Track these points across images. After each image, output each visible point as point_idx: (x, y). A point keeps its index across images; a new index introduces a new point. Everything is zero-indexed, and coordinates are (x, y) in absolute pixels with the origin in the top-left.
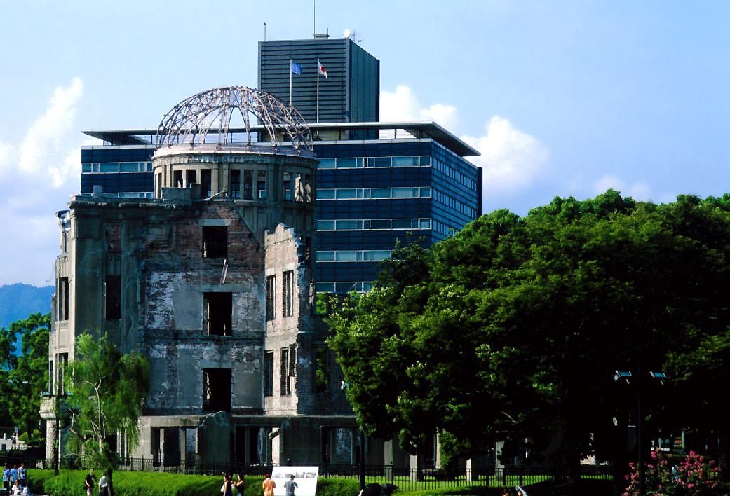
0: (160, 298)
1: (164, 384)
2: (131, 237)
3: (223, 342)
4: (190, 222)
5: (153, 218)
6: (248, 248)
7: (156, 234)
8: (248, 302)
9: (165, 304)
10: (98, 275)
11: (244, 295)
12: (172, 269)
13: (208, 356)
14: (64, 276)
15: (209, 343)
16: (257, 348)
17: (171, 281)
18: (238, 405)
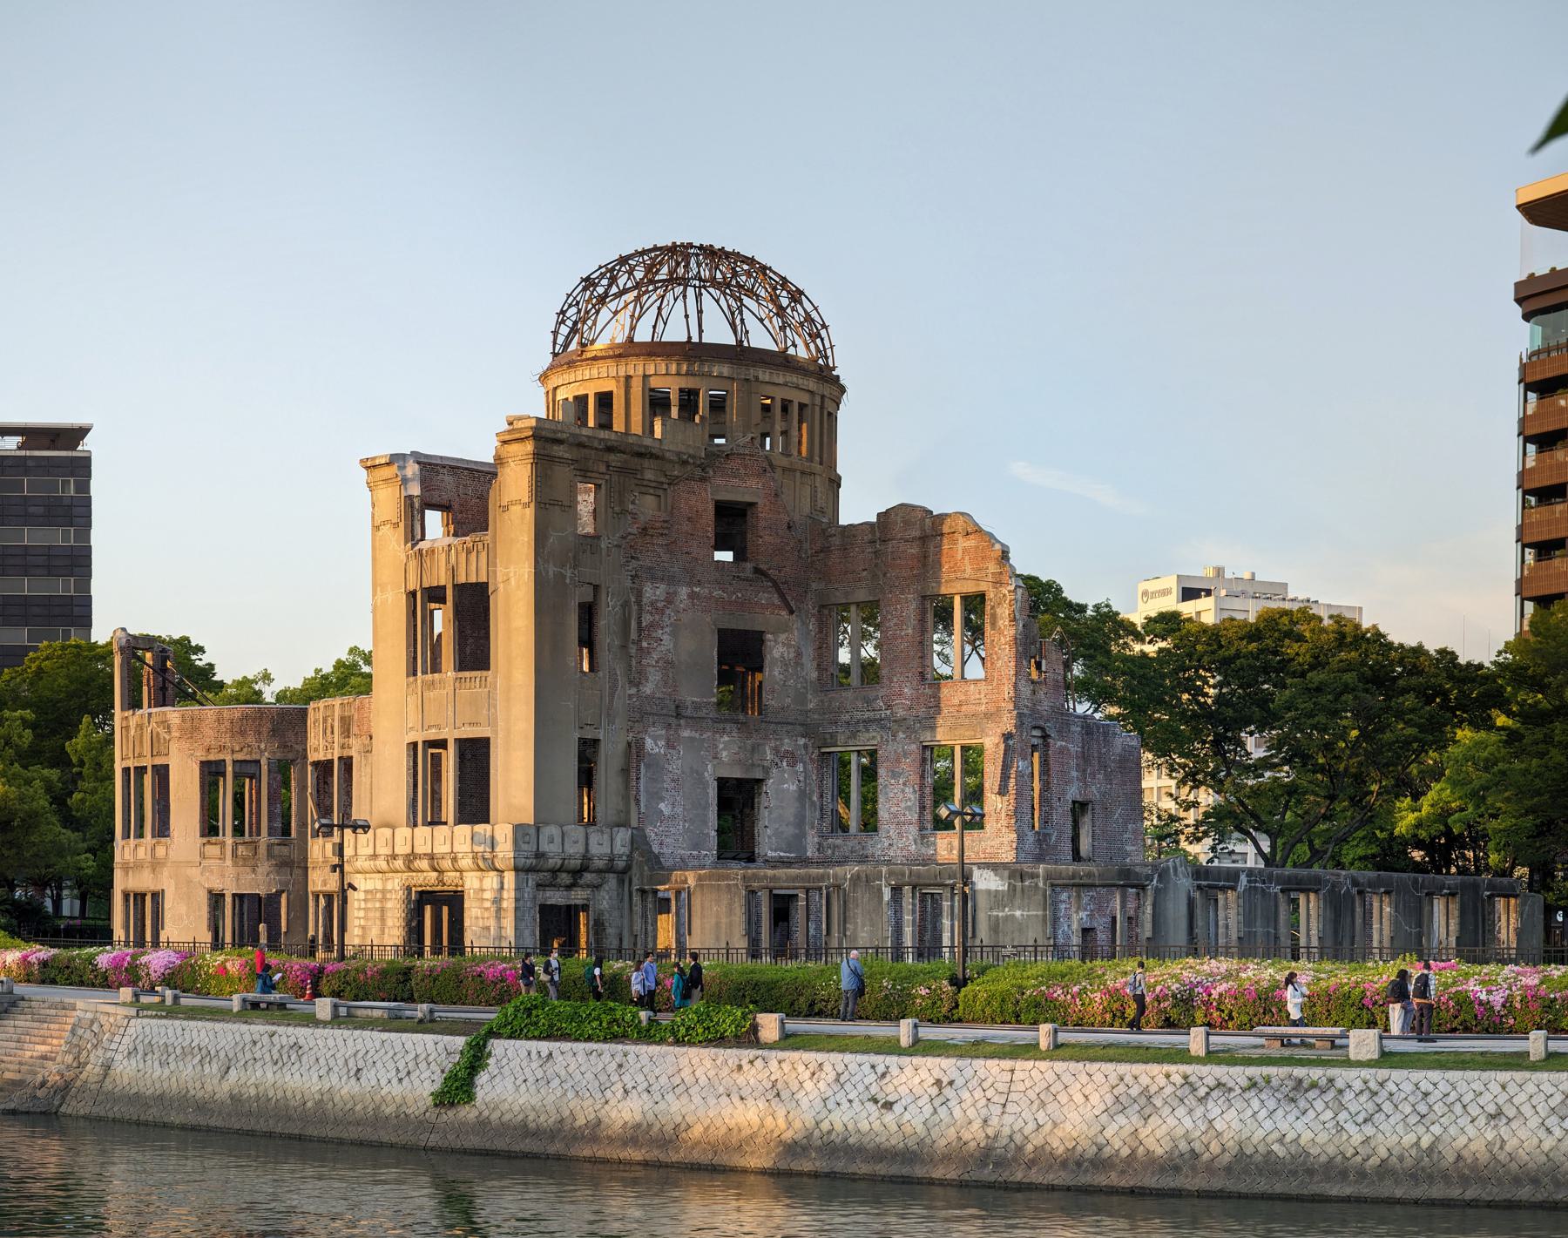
0: (654, 635)
1: (662, 806)
2: (617, 509)
3: (752, 727)
4: (695, 485)
5: (649, 475)
6: (788, 548)
7: (647, 507)
8: (789, 653)
9: (663, 648)
10: (568, 581)
11: (782, 637)
12: (671, 580)
13: (725, 754)
14: (473, 580)
15: (728, 726)
16: (802, 741)
17: (670, 602)
18: (775, 851)
